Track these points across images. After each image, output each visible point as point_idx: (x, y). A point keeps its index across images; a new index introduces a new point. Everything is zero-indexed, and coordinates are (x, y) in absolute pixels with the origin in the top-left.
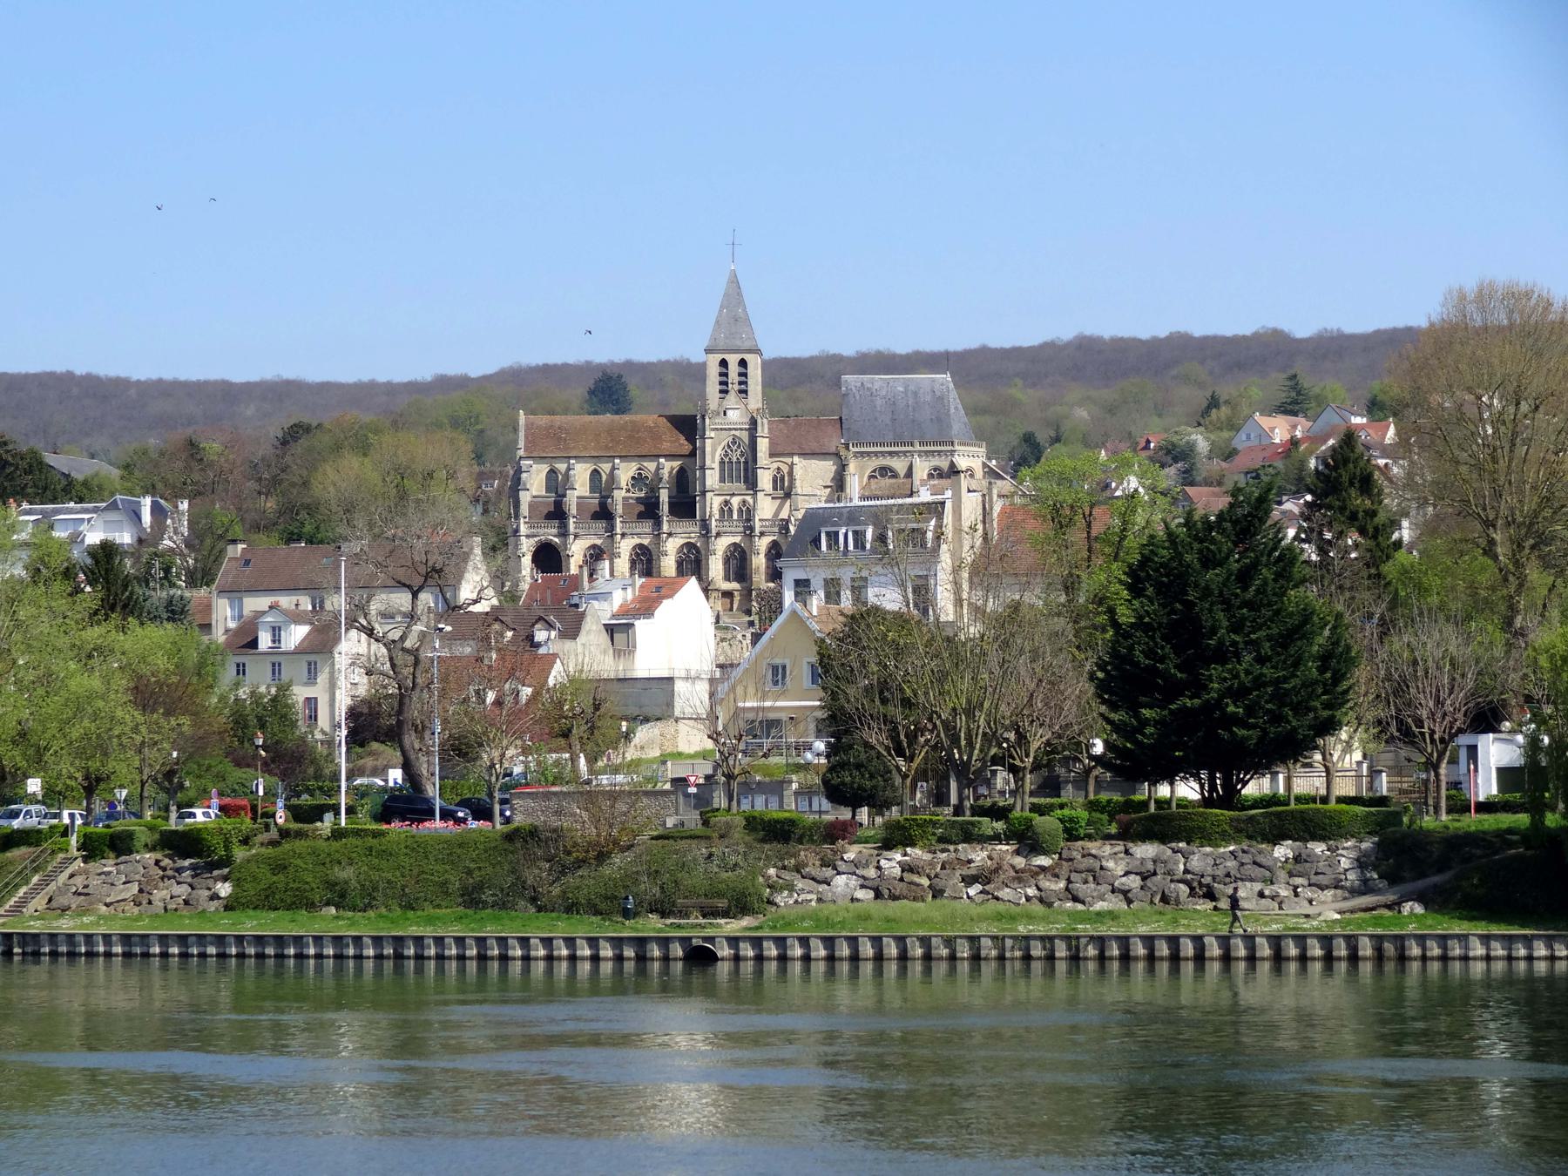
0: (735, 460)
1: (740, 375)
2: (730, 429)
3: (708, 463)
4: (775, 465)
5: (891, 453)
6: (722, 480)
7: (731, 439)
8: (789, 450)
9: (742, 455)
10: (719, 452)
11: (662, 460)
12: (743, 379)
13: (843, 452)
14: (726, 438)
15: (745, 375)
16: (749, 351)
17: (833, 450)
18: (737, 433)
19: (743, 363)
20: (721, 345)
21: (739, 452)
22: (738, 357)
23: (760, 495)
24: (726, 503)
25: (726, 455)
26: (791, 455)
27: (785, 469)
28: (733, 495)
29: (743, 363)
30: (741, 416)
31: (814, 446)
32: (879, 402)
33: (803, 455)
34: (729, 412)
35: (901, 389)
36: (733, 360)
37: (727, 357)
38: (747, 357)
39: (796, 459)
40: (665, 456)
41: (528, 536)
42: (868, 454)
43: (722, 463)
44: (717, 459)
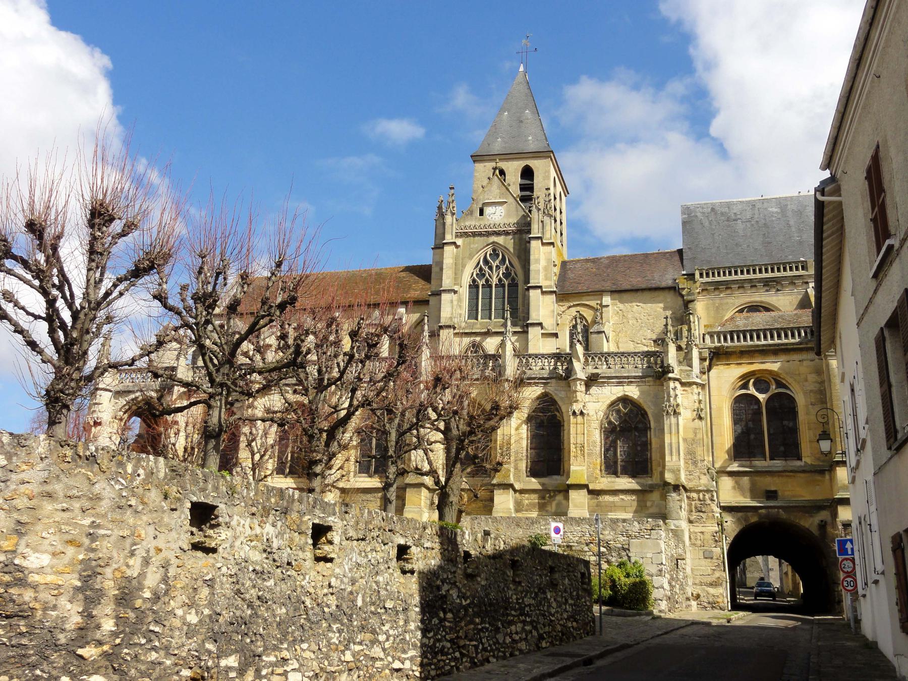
0: (495, 281)
1: (523, 188)
2: (488, 234)
3: (447, 282)
4: (573, 312)
5: (768, 283)
6: (473, 313)
7: (490, 251)
8: (598, 287)
9: (507, 275)
10: (468, 272)
11: (402, 310)
12: (528, 193)
13: (683, 284)
14: (480, 249)
15: (530, 188)
16: (537, 154)
17: (670, 283)
18: (500, 240)
19: (527, 173)
20: (498, 146)
21: (502, 270)
22: (520, 164)
23: (533, 332)
24: (476, 347)
25: (481, 274)
26: (600, 293)
27: (588, 314)
28: (488, 333)
29: (527, 173)
30: (508, 215)
31: (636, 281)
32: (740, 226)
33: (618, 292)
34: (488, 210)
35: (774, 210)
36: (514, 169)
37: (503, 165)
38: (534, 164)
39: (607, 300)
40: (405, 303)
41: (118, 394)
42: (727, 285)
43: (474, 286)
44: (466, 280)
